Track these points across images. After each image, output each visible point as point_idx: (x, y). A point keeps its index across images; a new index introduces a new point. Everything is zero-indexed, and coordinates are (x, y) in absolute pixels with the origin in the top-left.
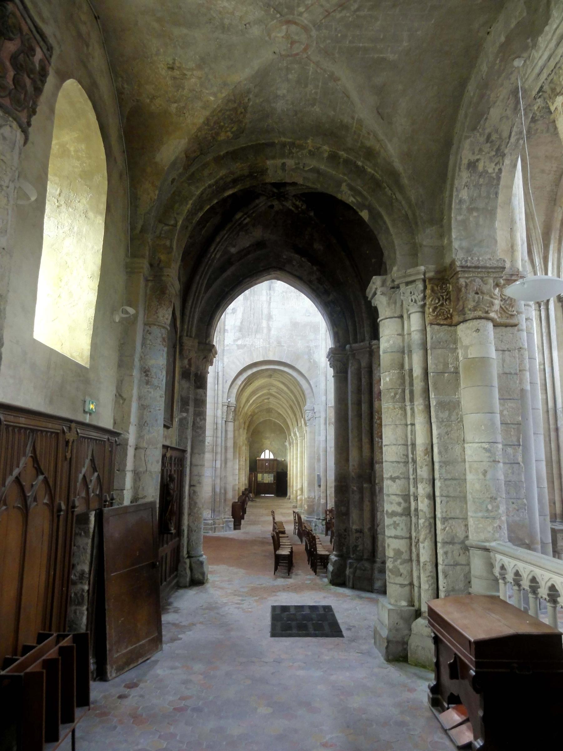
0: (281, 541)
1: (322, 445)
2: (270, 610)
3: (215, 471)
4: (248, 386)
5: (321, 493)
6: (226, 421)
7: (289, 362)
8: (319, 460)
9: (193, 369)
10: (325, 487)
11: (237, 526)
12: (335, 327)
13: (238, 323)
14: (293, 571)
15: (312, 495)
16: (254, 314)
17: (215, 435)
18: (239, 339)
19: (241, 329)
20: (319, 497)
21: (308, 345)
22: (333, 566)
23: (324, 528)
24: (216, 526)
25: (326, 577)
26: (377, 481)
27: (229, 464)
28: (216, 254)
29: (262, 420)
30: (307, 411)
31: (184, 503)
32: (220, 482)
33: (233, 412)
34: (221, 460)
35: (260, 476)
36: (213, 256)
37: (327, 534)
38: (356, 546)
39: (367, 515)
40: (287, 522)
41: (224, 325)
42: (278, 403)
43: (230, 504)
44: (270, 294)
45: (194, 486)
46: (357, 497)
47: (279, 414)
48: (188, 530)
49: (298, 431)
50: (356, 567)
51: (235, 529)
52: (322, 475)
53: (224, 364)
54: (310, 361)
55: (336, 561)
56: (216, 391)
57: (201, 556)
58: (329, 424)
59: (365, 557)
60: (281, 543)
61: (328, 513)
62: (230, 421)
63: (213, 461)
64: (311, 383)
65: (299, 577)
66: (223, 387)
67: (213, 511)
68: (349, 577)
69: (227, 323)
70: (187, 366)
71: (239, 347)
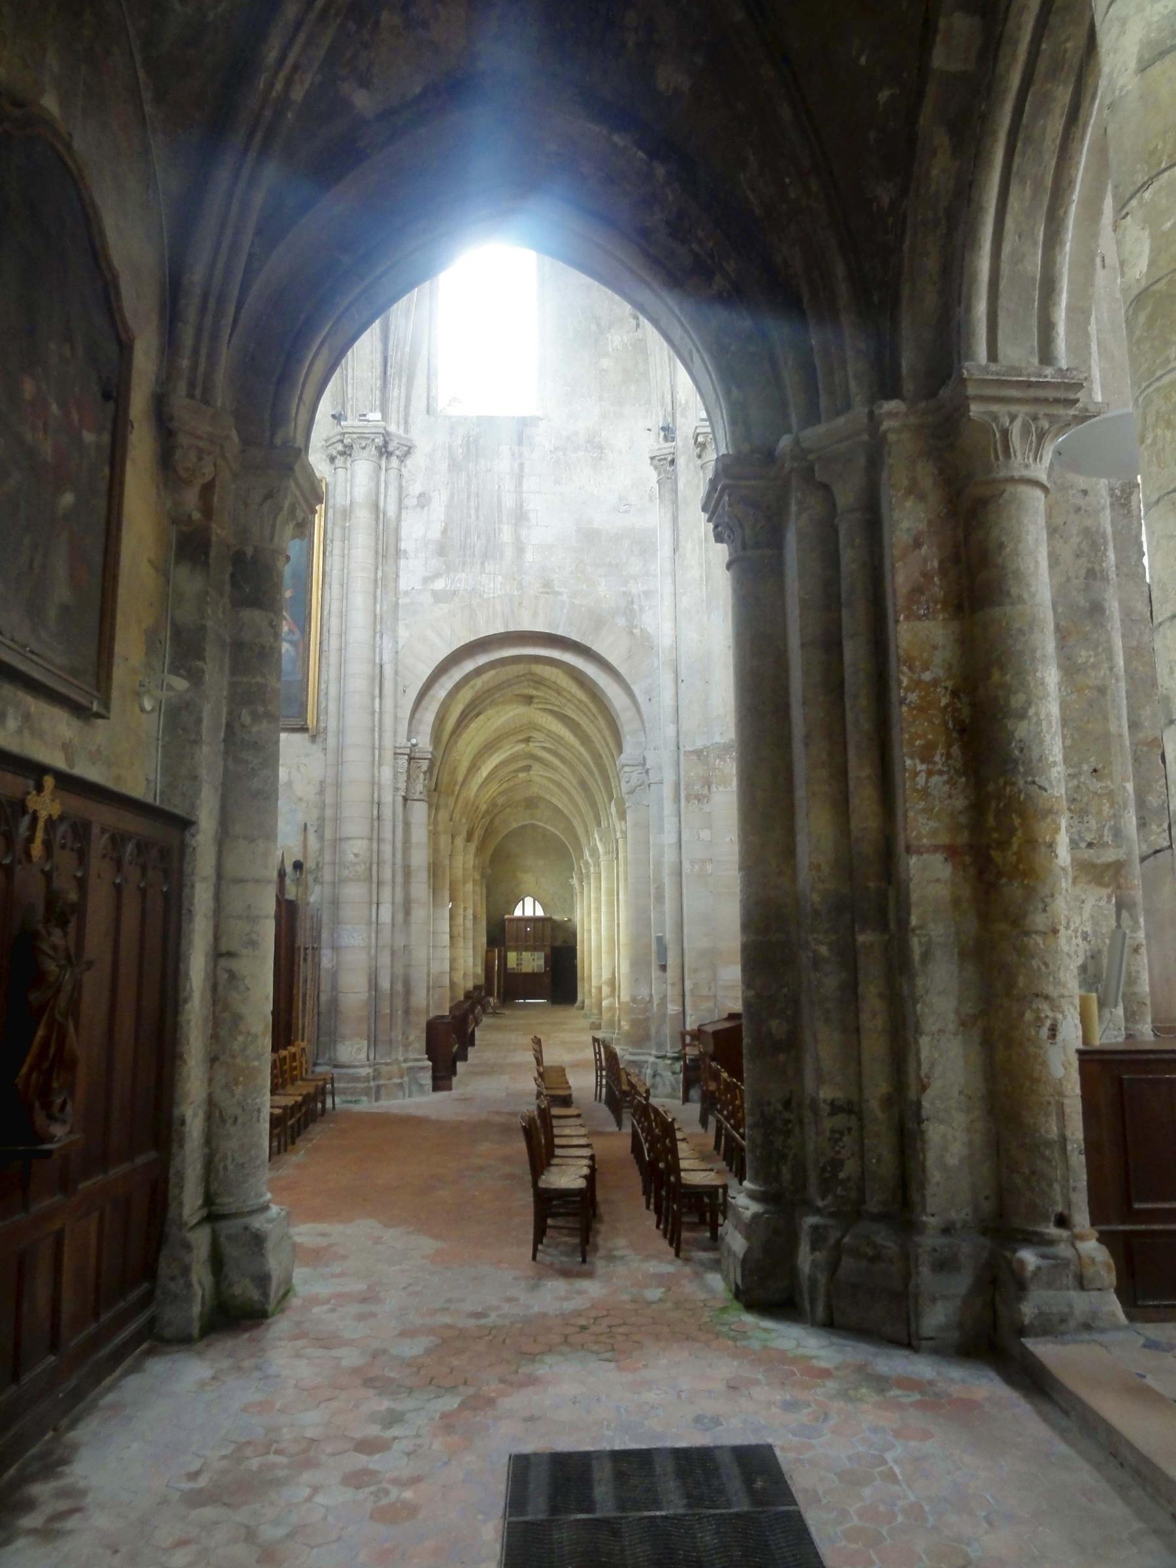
0: (556, 1131)
1: (669, 857)
2: (498, 1486)
3: (377, 932)
4: (472, 720)
5: (669, 987)
6: (405, 799)
7: (574, 637)
8: (660, 898)
9: (221, 532)
10: (680, 970)
11: (442, 1078)
12: (735, 390)
13: (435, 533)
14: (600, 1241)
15: (643, 992)
16: (477, 509)
17: (375, 836)
18: (437, 575)
19: (442, 550)
20: (663, 998)
21: (624, 589)
22: (748, 1238)
23: (677, 1082)
24: (382, 1082)
25: (716, 1265)
26: (914, 921)
27: (419, 914)
28: (289, 83)
29: (514, 825)
30: (626, 769)
31: (183, 1019)
32: (392, 960)
33: (425, 773)
34: (393, 903)
35: (512, 957)
36: (279, 86)
37: (686, 1099)
38: (836, 1164)
39: (874, 1046)
40: (576, 1065)
41: (398, 539)
42: (550, 779)
43: (423, 1022)
44: (521, 455)
45: (230, 955)
46: (830, 982)
47: (556, 809)
48: (209, 1117)
49: (601, 840)
50: (838, 1243)
51: (436, 1088)
52: (669, 937)
53: (397, 643)
54: (632, 633)
55: (756, 1216)
56: (377, 715)
57: (265, 1208)
58: (688, 800)
59: (873, 1205)
60: (557, 1141)
61: (688, 1039)
62: (417, 796)
63: (371, 904)
64: (636, 689)
65: (621, 1269)
66: (396, 707)
67: (374, 1041)
68: (813, 1281)
69: (404, 534)
70: (196, 516)
71: (438, 597)
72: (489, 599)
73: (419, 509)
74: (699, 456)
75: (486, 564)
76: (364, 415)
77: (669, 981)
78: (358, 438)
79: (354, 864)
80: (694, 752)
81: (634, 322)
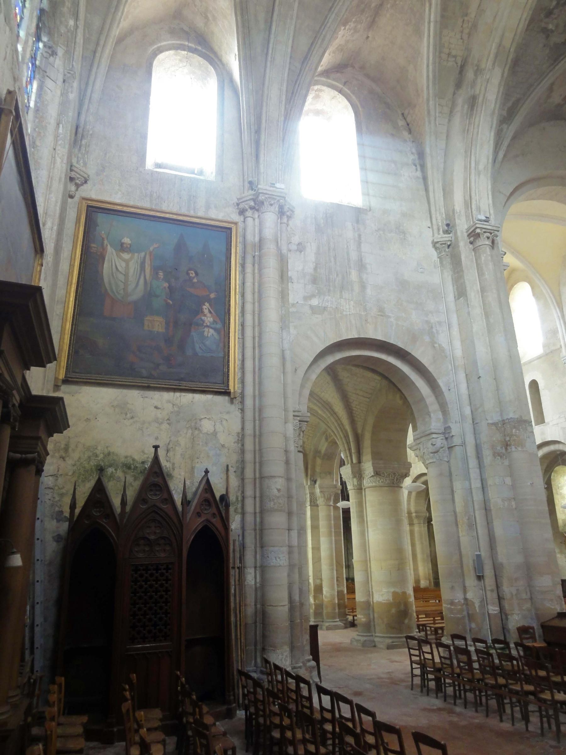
13: (310, 268)
16: (335, 258)
18: (313, 296)
19: (314, 281)
21: (426, 319)
44: (359, 229)
54: (434, 347)
71: (314, 310)
72: (346, 315)
73: (298, 253)
74: (471, 243)
75: (343, 293)
76: (274, 184)
77: (488, 588)
78: (269, 198)
79: (278, 497)
80: (493, 424)
81: (414, 167)
